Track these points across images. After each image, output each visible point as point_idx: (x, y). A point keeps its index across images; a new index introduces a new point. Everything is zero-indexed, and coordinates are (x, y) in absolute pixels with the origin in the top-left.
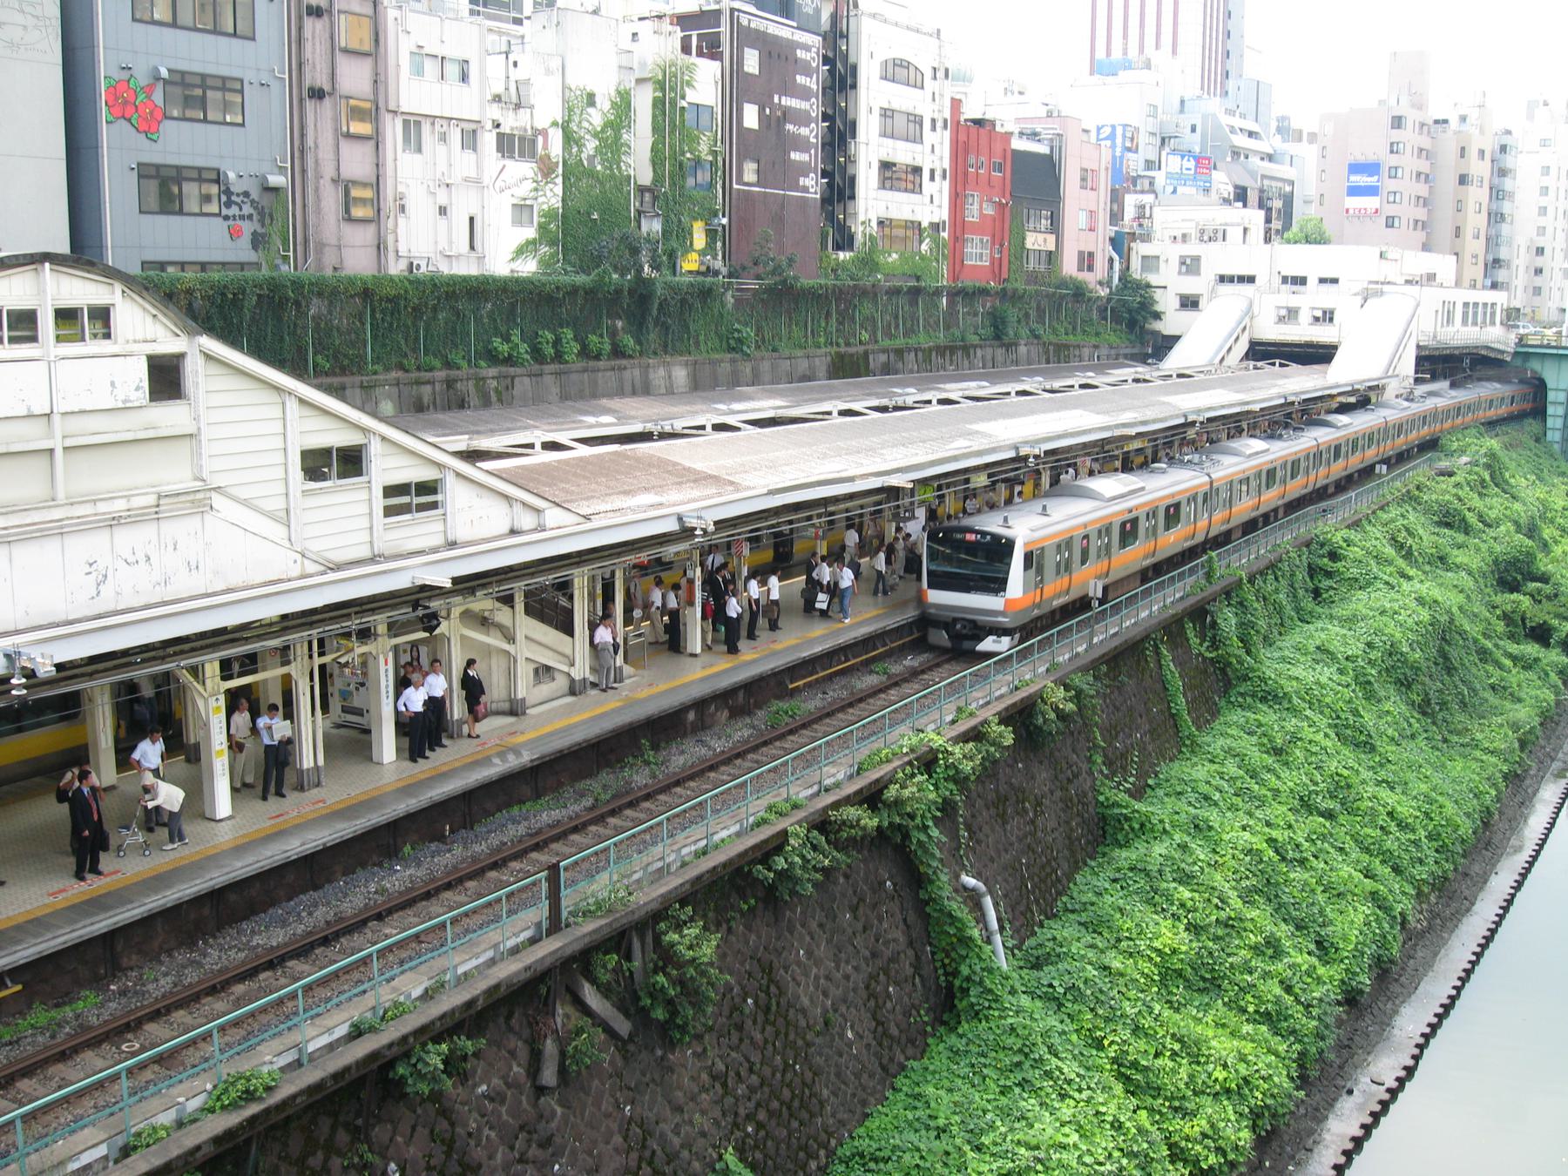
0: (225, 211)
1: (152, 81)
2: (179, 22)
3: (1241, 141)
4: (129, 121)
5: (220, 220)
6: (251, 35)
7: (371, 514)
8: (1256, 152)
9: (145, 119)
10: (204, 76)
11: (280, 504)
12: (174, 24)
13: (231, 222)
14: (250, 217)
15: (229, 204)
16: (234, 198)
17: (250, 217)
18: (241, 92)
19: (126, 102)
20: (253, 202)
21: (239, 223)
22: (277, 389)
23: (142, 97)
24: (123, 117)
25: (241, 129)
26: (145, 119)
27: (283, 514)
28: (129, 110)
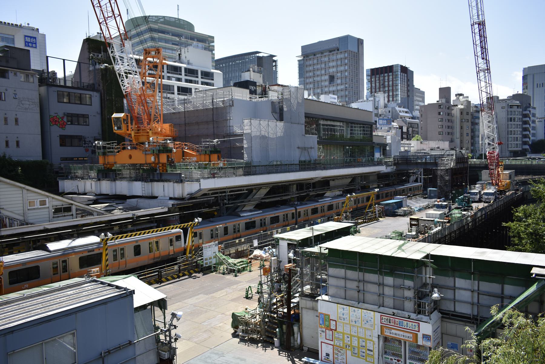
0: (84, 145)
1: (63, 116)
2: (71, 102)
3: (401, 114)
4: (57, 125)
6: (90, 104)
7: (49, 214)
8: (407, 117)
9: (61, 125)
10: (78, 115)
11: (22, 212)
12: (69, 103)
13: (85, 148)
14: (91, 147)
15: (85, 144)
16: (86, 142)
18: (88, 118)
19: (56, 121)
21: (88, 148)
22: (21, 187)
23: (60, 120)
24: (55, 124)
26: (61, 125)
27: (22, 214)
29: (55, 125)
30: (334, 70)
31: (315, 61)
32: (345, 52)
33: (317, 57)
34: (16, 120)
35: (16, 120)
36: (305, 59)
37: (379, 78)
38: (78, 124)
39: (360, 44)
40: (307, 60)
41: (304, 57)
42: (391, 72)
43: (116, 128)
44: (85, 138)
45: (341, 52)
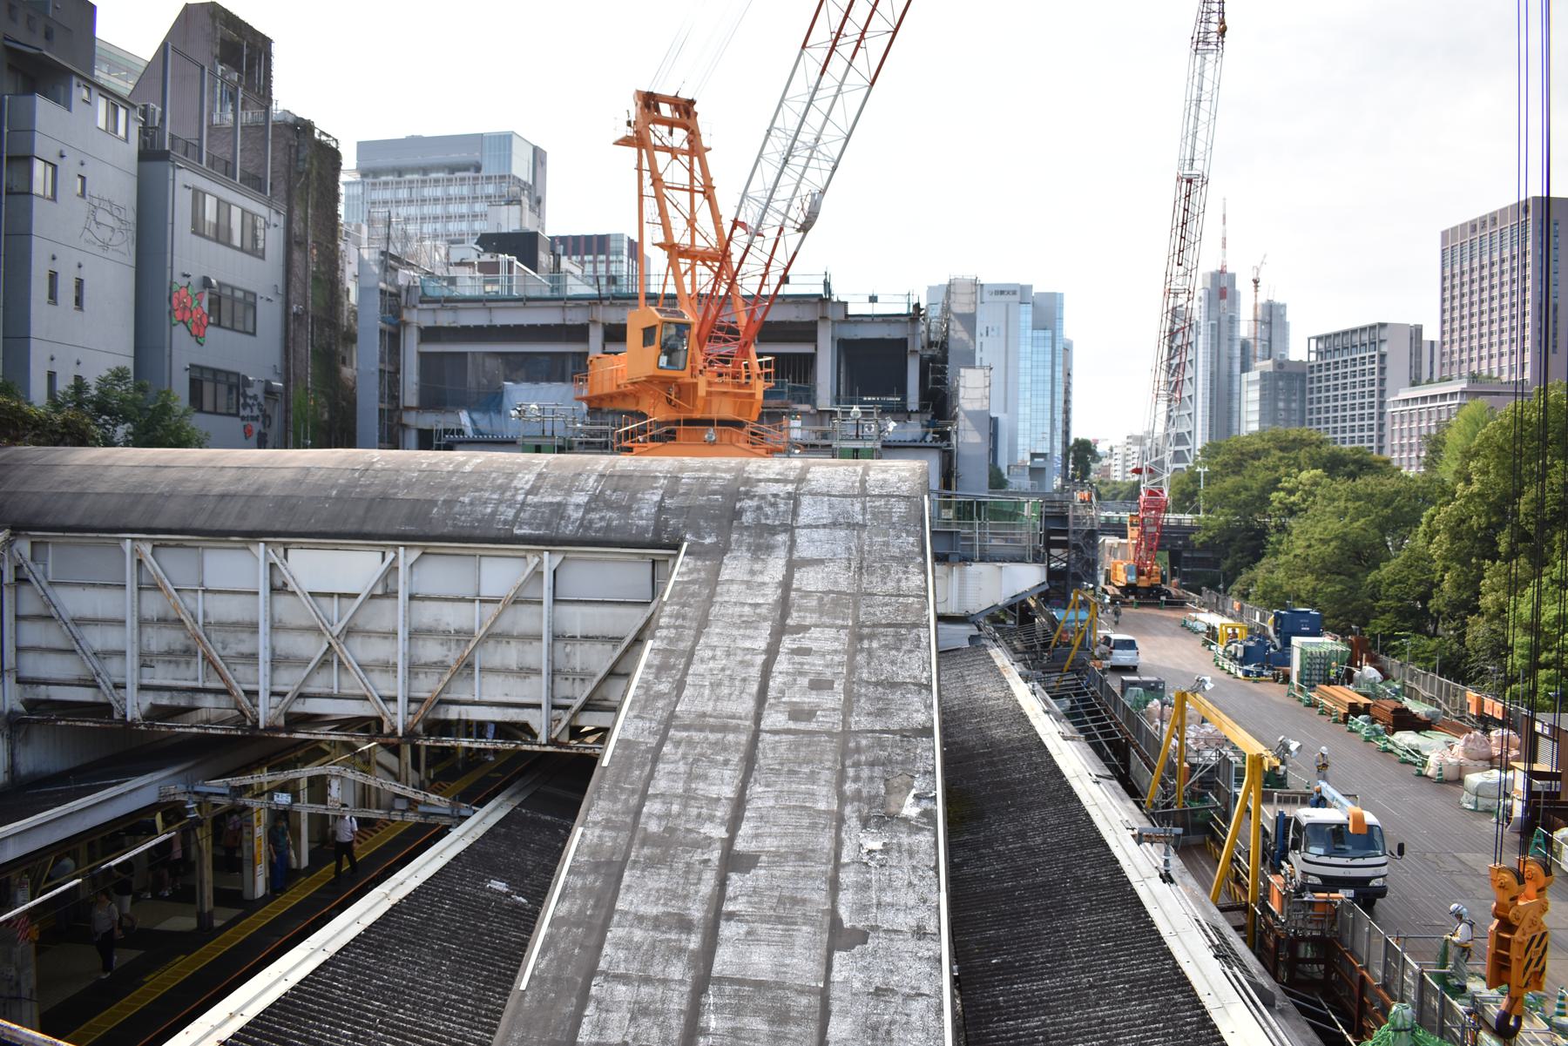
5: (238, 420)
13: (245, 423)
14: (255, 419)
15: (245, 405)
17: (255, 419)
20: (259, 404)
21: (251, 423)
23: (196, 303)
25: (251, 338)
28: (187, 315)
29: (182, 325)
30: (464, 226)
31: (403, 194)
32: (502, 177)
33: (411, 182)
34: (80, 284)
35: (80, 284)
36: (370, 180)
37: (594, 262)
38: (232, 329)
39: (538, 163)
40: (374, 184)
41: (364, 175)
42: (603, 253)
43: (664, 360)
44: (247, 383)
45: (489, 178)
